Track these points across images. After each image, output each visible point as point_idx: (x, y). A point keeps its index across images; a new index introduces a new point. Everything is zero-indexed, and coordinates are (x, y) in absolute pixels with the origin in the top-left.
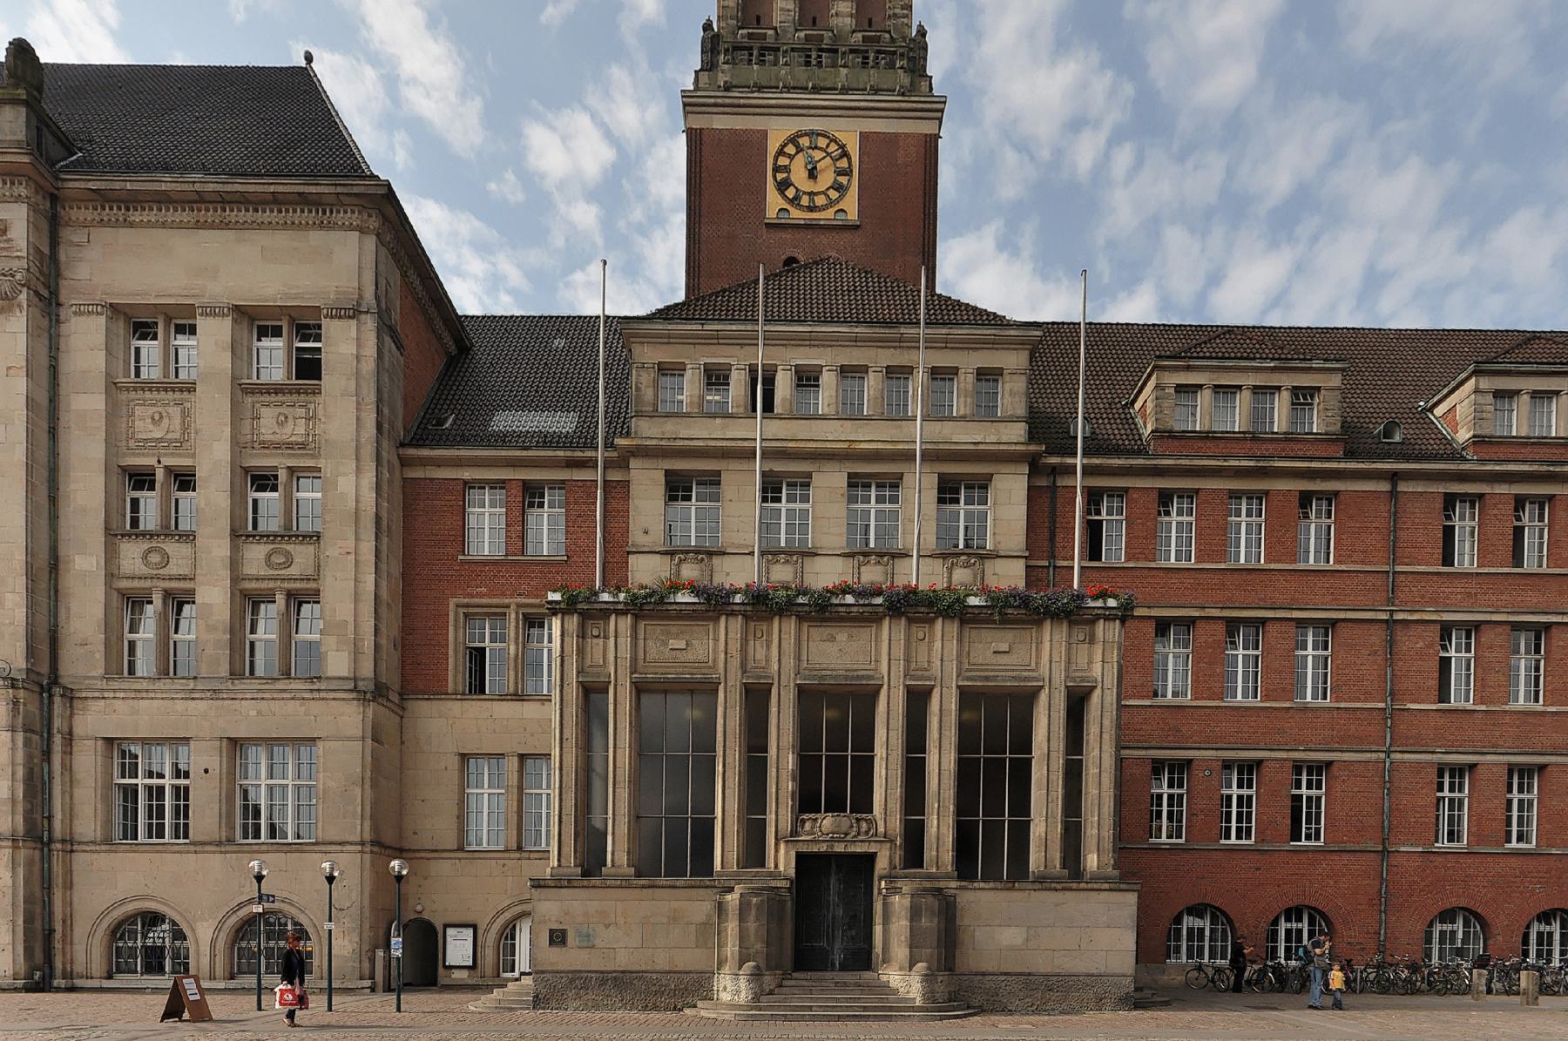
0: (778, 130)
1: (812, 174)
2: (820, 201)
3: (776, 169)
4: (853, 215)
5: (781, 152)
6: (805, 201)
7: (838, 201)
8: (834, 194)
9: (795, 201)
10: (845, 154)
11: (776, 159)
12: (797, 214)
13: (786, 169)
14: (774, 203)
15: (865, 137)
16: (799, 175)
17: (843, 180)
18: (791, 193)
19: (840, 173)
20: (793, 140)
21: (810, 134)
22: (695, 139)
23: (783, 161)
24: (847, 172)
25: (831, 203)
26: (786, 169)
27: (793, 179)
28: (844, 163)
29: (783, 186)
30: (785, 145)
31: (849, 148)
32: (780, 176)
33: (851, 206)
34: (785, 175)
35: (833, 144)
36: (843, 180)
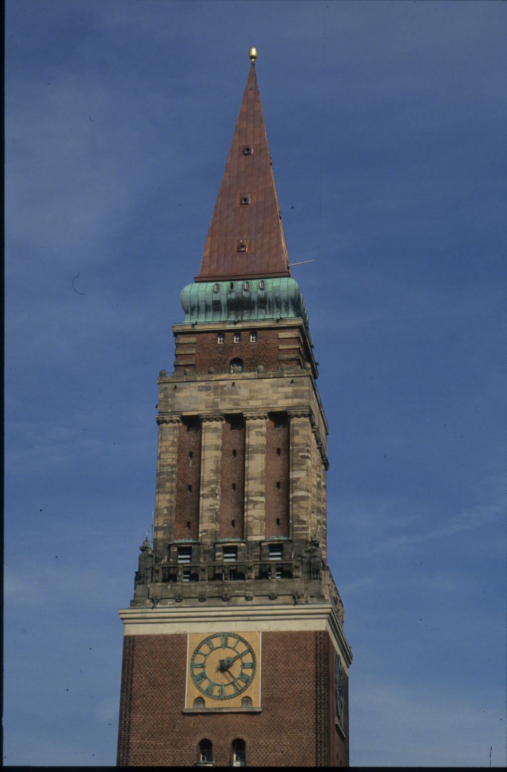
3: (193, 666)
5: (197, 652)
6: (216, 692)
7: (243, 690)
10: (250, 650)
11: (193, 660)
12: (210, 704)
13: (203, 666)
14: (191, 692)
16: (211, 670)
17: (248, 672)
18: (205, 685)
20: (208, 640)
21: (226, 636)
23: (200, 659)
24: (253, 666)
25: (239, 692)
26: (203, 666)
27: (207, 674)
28: (248, 659)
30: (199, 647)
31: (254, 648)
32: (197, 672)
33: (255, 693)
34: (201, 670)
35: (240, 643)
36: (248, 672)
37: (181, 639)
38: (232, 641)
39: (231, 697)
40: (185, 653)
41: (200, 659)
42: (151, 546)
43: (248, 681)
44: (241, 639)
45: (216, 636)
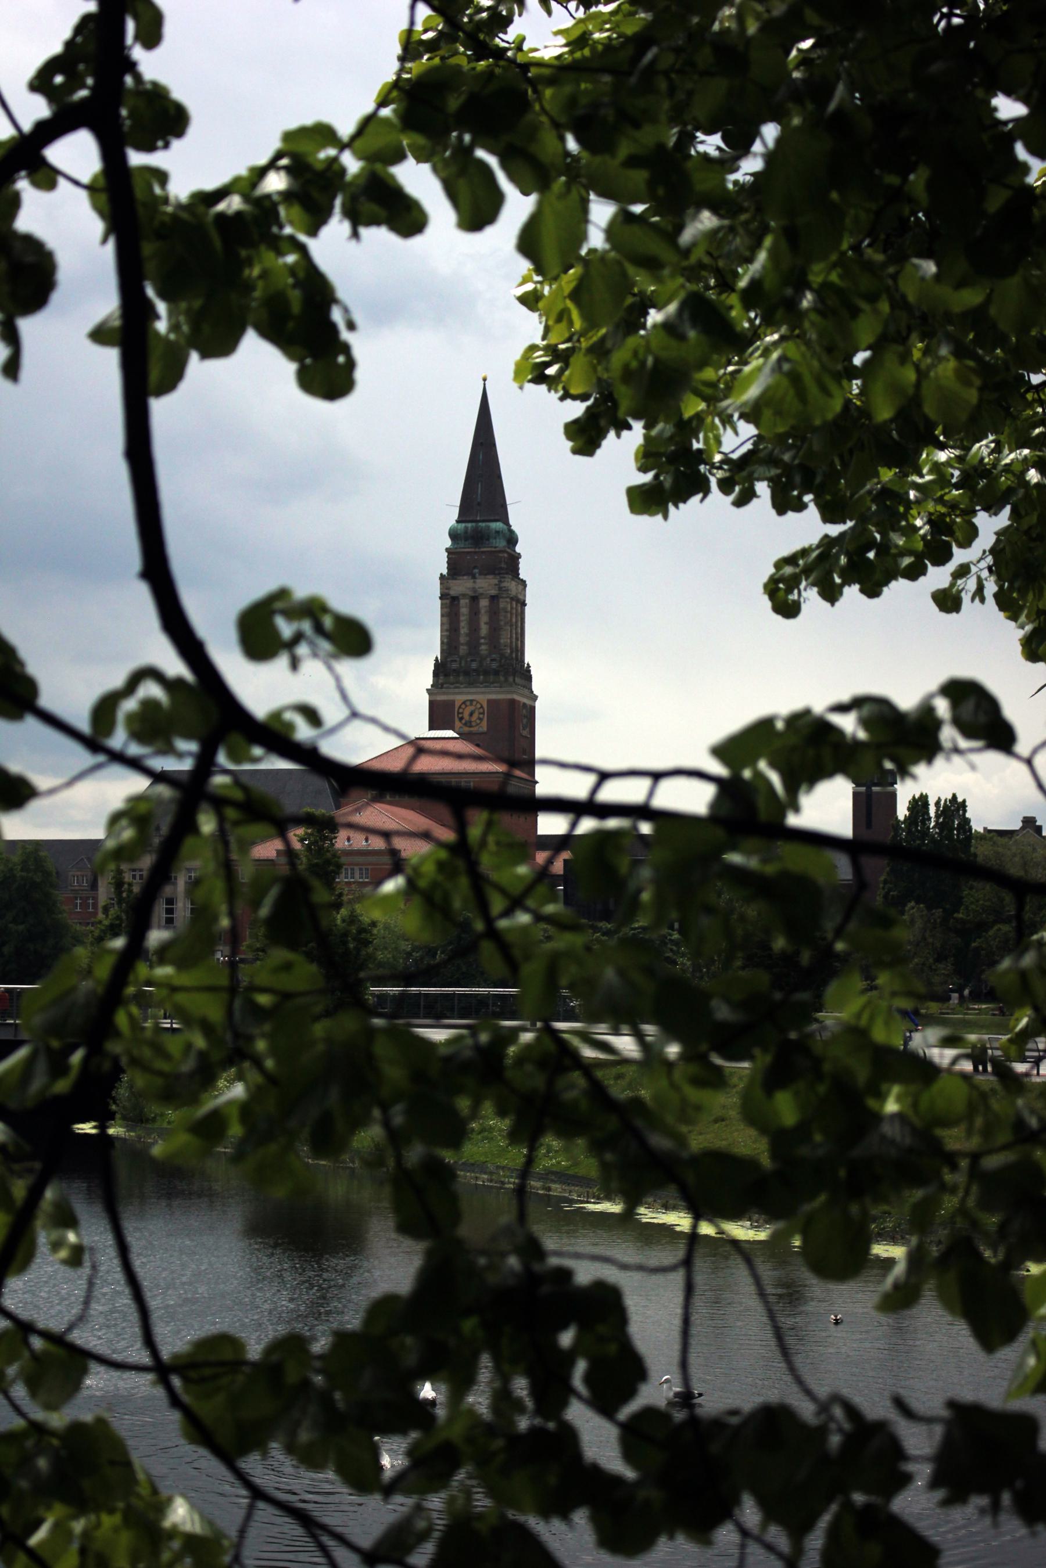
0: (459, 699)
1: (471, 714)
2: (474, 724)
4: (485, 729)
5: (460, 707)
6: (468, 724)
8: (478, 721)
9: (465, 724)
10: (482, 707)
13: (462, 713)
15: (489, 701)
17: (481, 716)
18: (463, 721)
19: (480, 713)
20: (464, 703)
21: (472, 701)
22: (432, 704)
23: (461, 711)
24: (483, 713)
25: (478, 724)
28: (481, 710)
29: (461, 719)
32: (460, 716)
33: (485, 723)
36: (481, 716)
37: (453, 703)
38: (474, 703)
39: (476, 726)
40: (455, 708)
41: (461, 711)
42: (439, 658)
43: (481, 719)
44: (478, 702)
45: (467, 700)
